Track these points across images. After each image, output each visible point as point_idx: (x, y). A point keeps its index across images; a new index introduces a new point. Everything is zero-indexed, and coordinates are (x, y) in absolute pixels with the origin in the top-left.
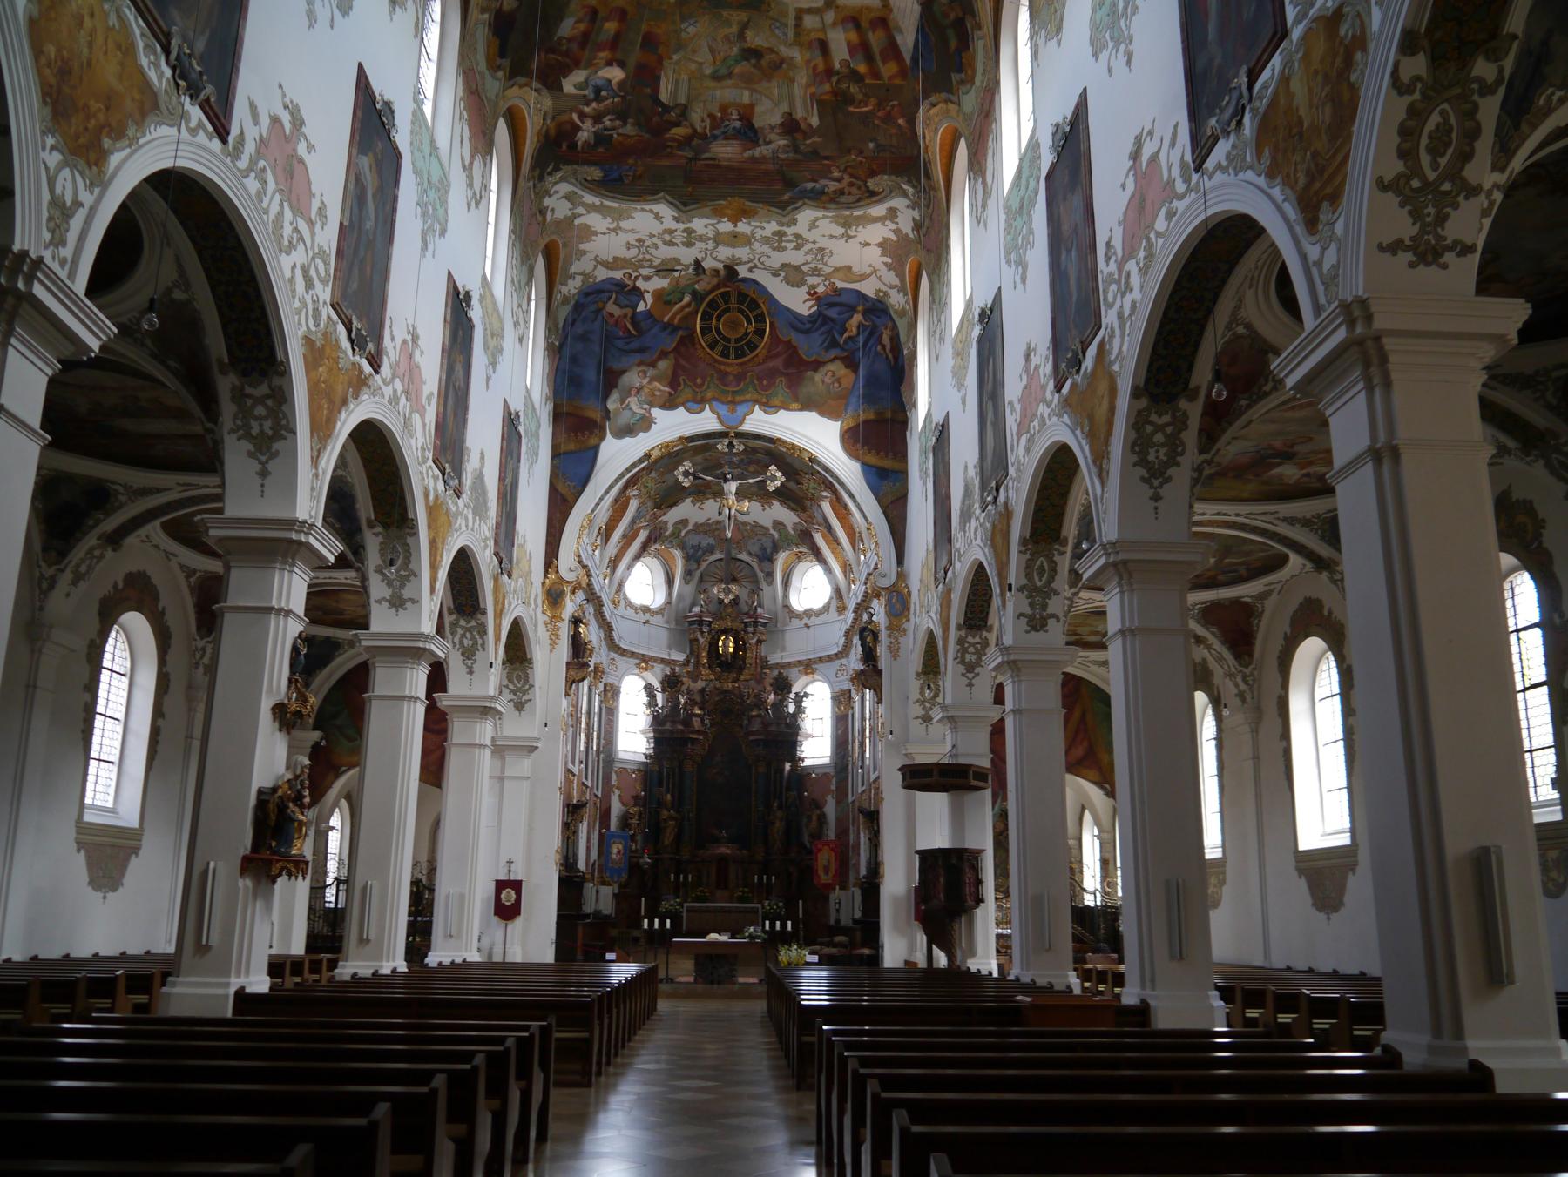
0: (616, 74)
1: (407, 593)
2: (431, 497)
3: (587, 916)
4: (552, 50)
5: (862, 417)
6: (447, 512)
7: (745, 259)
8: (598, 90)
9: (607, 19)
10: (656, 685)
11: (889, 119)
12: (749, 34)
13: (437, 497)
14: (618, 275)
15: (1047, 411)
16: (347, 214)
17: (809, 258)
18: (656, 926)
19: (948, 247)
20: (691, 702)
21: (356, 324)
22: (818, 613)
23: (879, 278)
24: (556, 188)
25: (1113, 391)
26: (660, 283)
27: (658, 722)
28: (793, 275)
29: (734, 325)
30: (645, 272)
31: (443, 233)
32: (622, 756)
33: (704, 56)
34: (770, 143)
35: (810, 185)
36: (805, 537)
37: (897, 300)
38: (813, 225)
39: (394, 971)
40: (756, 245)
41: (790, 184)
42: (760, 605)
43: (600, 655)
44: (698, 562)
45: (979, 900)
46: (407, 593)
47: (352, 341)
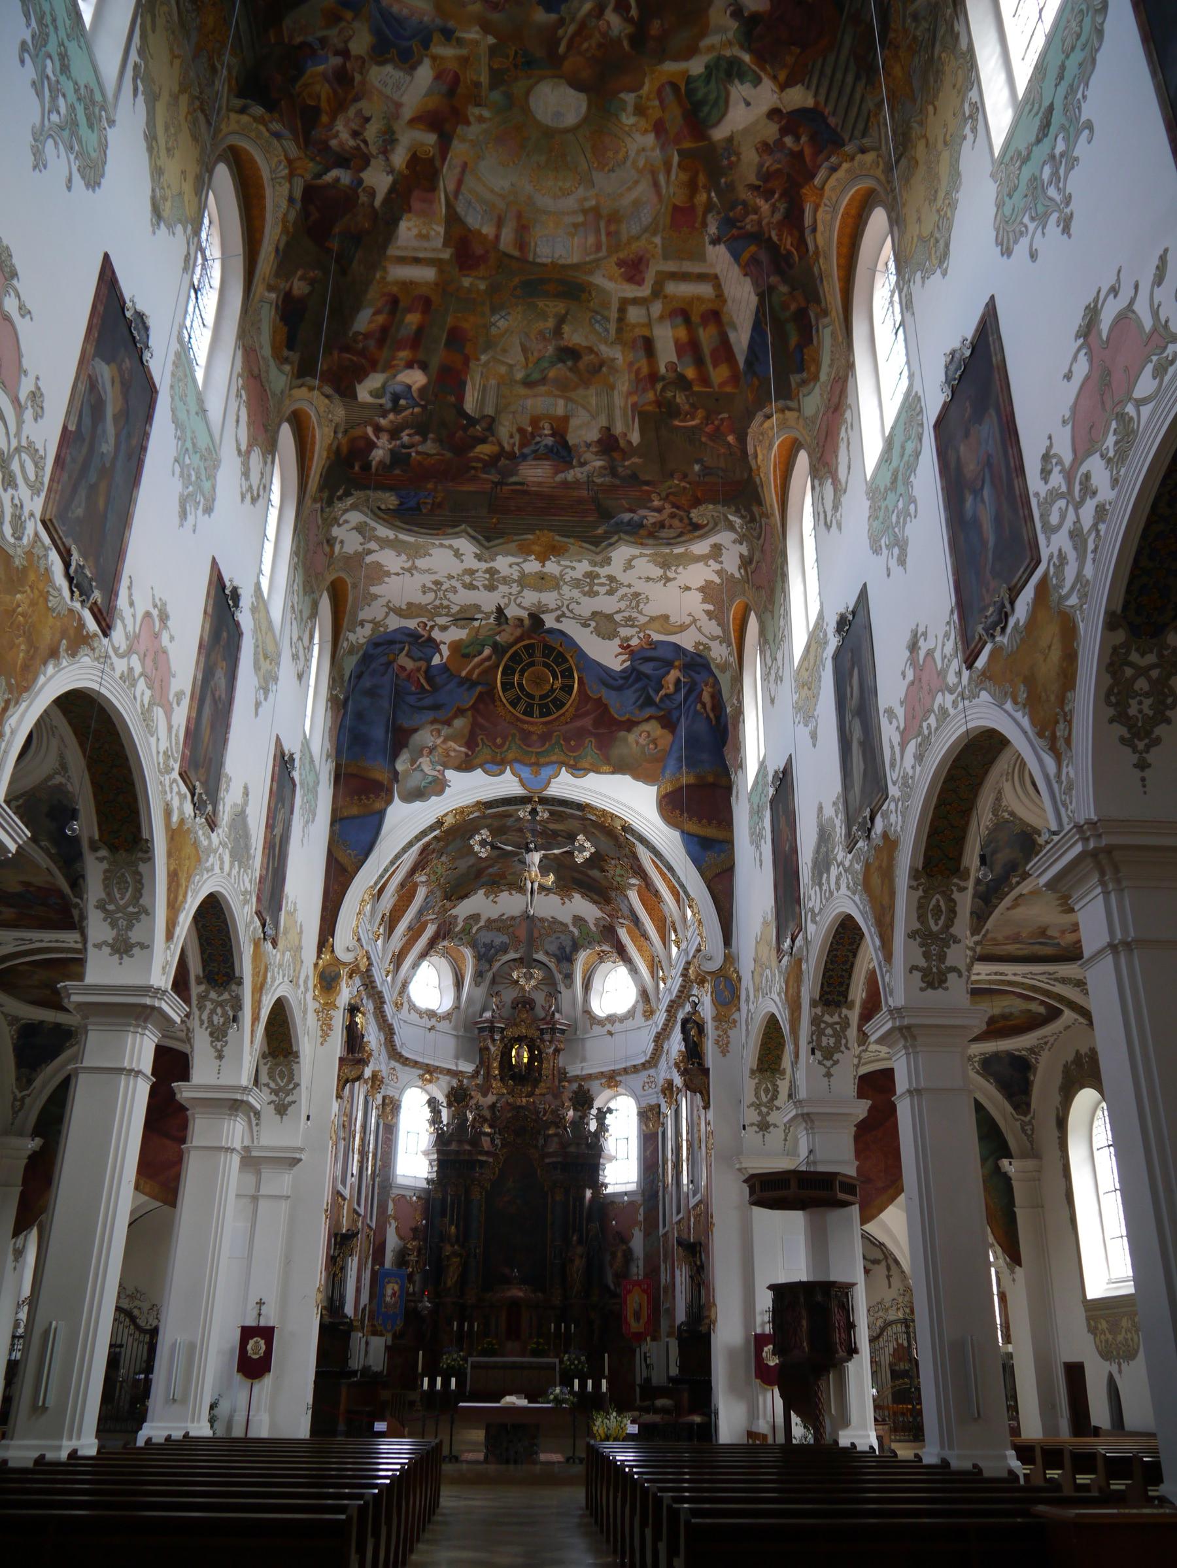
0: (416, 378)
1: (135, 936)
2: (175, 818)
3: (354, 1373)
4: (346, 348)
5: (684, 781)
6: (196, 844)
7: (552, 606)
8: (396, 398)
9: (409, 310)
10: (441, 1098)
11: (717, 436)
12: (566, 329)
13: (182, 821)
14: (412, 624)
15: (949, 698)
16: (74, 419)
17: (623, 605)
18: (439, 1386)
19: (784, 576)
20: (480, 1119)
21: (75, 557)
23: (699, 629)
24: (346, 516)
25: (1069, 631)
26: (458, 634)
27: (443, 1142)
28: (604, 624)
29: (538, 681)
30: (442, 621)
31: (208, 510)
32: (400, 1181)
33: (515, 356)
34: (582, 465)
35: (627, 516)
36: (608, 932)
37: (719, 653)
38: (629, 566)
39: (73, 1455)
40: (565, 589)
41: (605, 515)
42: (558, 1010)
43: (378, 1063)
44: (490, 962)
45: (853, 1351)
46: (135, 936)
47: (70, 579)
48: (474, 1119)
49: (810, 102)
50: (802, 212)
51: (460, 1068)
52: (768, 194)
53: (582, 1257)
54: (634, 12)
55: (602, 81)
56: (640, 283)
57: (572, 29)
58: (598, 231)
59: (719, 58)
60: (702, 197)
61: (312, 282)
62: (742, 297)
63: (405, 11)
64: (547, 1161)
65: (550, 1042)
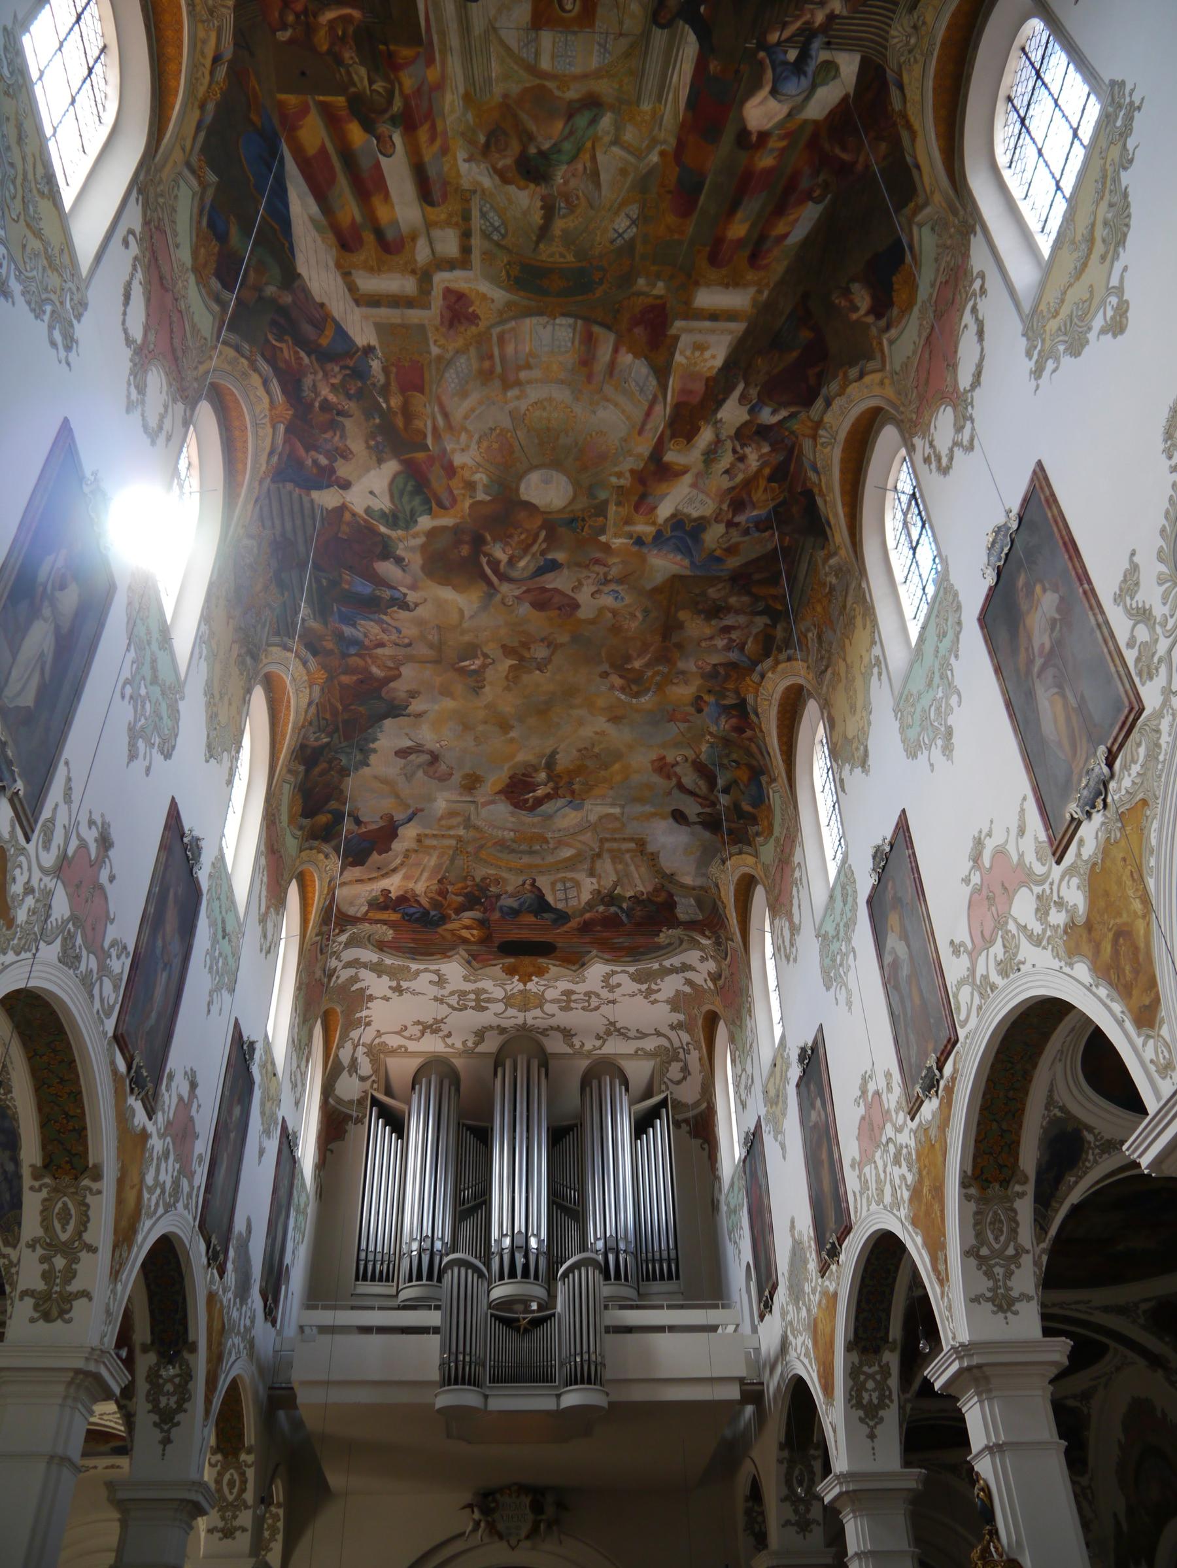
0: (762, 111)
9: (740, 243)
12: (537, 218)
33: (610, 160)
49: (315, 495)
50: (284, 392)
52: (326, 406)
54: (484, 560)
55: (506, 511)
56: (448, 291)
57: (535, 548)
58: (503, 358)
59: (407, 528)
60: (395, 402)
61: (847, 292)
62: (317, 270)
63: (671, 556)
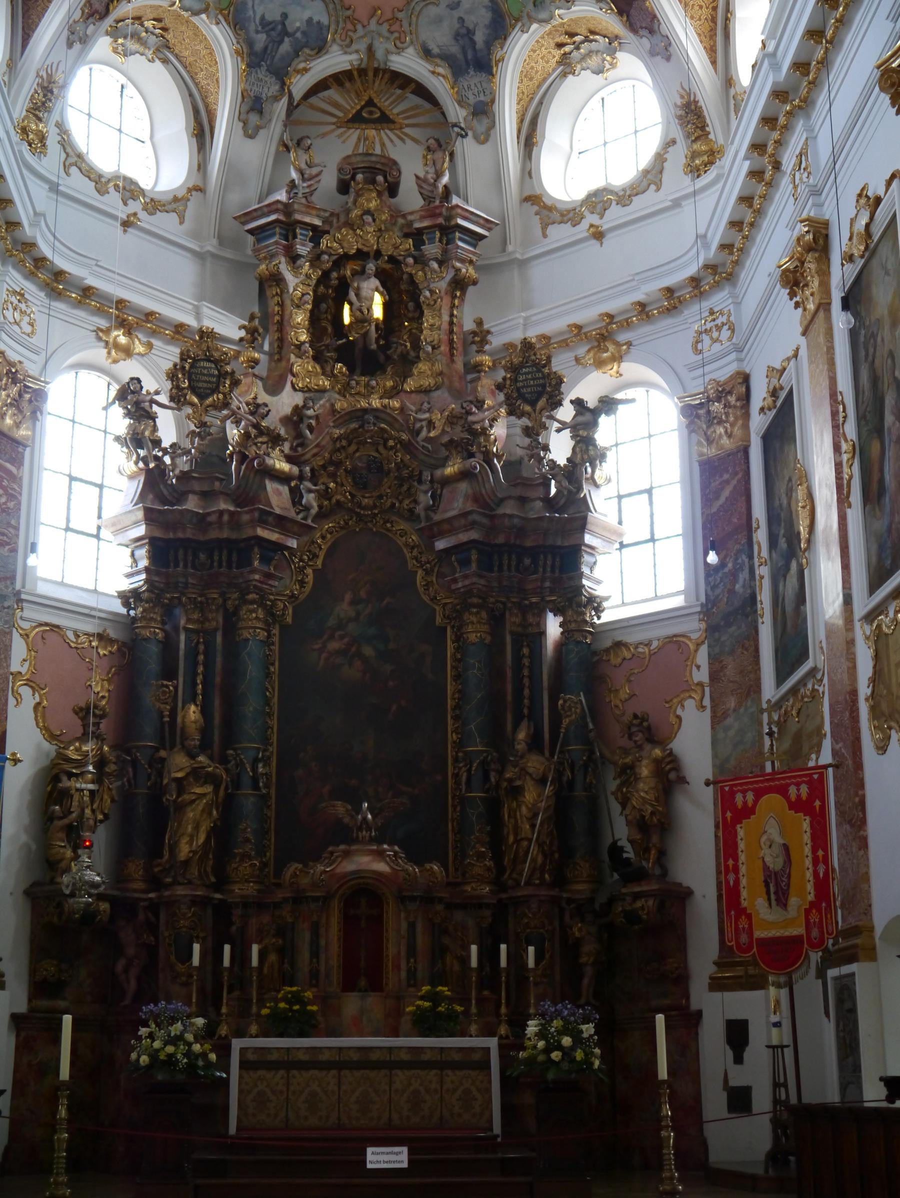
10: (153, 383)
20: (259, 433)
22: (626, 196)
27: (160, 490)
32: (43, 589)
44: (281, 75)
48: (246, 436)
51: (208, 324)
53: (542, 781)
64: (441, 545)
65: (441, 263)
